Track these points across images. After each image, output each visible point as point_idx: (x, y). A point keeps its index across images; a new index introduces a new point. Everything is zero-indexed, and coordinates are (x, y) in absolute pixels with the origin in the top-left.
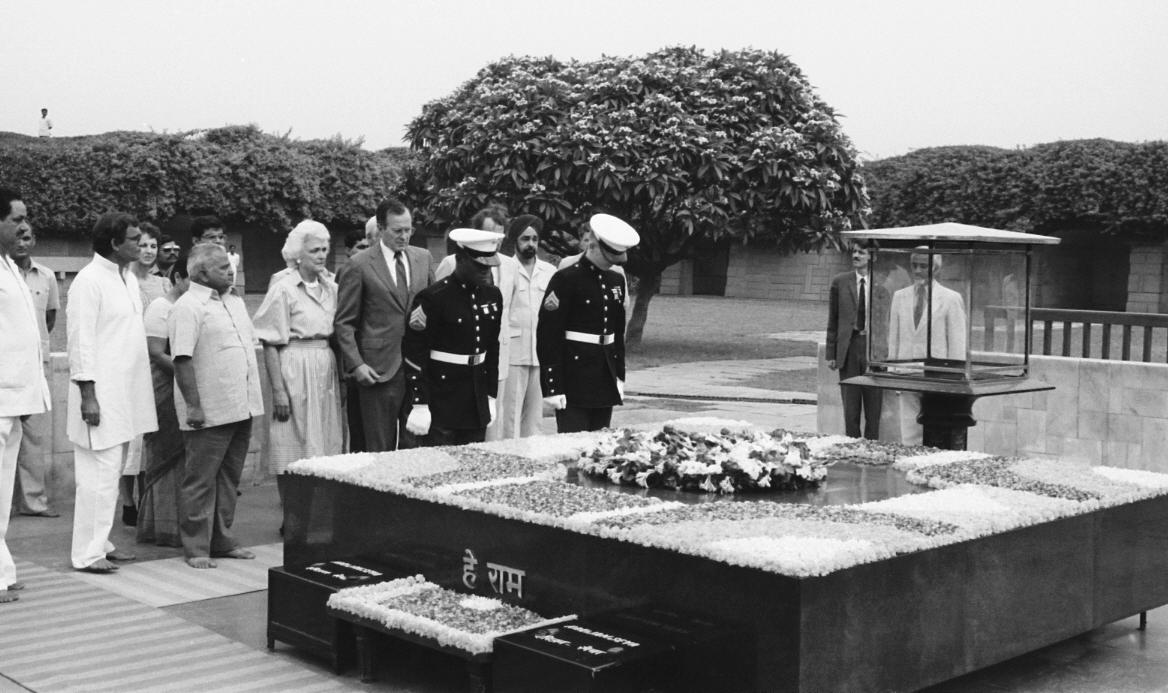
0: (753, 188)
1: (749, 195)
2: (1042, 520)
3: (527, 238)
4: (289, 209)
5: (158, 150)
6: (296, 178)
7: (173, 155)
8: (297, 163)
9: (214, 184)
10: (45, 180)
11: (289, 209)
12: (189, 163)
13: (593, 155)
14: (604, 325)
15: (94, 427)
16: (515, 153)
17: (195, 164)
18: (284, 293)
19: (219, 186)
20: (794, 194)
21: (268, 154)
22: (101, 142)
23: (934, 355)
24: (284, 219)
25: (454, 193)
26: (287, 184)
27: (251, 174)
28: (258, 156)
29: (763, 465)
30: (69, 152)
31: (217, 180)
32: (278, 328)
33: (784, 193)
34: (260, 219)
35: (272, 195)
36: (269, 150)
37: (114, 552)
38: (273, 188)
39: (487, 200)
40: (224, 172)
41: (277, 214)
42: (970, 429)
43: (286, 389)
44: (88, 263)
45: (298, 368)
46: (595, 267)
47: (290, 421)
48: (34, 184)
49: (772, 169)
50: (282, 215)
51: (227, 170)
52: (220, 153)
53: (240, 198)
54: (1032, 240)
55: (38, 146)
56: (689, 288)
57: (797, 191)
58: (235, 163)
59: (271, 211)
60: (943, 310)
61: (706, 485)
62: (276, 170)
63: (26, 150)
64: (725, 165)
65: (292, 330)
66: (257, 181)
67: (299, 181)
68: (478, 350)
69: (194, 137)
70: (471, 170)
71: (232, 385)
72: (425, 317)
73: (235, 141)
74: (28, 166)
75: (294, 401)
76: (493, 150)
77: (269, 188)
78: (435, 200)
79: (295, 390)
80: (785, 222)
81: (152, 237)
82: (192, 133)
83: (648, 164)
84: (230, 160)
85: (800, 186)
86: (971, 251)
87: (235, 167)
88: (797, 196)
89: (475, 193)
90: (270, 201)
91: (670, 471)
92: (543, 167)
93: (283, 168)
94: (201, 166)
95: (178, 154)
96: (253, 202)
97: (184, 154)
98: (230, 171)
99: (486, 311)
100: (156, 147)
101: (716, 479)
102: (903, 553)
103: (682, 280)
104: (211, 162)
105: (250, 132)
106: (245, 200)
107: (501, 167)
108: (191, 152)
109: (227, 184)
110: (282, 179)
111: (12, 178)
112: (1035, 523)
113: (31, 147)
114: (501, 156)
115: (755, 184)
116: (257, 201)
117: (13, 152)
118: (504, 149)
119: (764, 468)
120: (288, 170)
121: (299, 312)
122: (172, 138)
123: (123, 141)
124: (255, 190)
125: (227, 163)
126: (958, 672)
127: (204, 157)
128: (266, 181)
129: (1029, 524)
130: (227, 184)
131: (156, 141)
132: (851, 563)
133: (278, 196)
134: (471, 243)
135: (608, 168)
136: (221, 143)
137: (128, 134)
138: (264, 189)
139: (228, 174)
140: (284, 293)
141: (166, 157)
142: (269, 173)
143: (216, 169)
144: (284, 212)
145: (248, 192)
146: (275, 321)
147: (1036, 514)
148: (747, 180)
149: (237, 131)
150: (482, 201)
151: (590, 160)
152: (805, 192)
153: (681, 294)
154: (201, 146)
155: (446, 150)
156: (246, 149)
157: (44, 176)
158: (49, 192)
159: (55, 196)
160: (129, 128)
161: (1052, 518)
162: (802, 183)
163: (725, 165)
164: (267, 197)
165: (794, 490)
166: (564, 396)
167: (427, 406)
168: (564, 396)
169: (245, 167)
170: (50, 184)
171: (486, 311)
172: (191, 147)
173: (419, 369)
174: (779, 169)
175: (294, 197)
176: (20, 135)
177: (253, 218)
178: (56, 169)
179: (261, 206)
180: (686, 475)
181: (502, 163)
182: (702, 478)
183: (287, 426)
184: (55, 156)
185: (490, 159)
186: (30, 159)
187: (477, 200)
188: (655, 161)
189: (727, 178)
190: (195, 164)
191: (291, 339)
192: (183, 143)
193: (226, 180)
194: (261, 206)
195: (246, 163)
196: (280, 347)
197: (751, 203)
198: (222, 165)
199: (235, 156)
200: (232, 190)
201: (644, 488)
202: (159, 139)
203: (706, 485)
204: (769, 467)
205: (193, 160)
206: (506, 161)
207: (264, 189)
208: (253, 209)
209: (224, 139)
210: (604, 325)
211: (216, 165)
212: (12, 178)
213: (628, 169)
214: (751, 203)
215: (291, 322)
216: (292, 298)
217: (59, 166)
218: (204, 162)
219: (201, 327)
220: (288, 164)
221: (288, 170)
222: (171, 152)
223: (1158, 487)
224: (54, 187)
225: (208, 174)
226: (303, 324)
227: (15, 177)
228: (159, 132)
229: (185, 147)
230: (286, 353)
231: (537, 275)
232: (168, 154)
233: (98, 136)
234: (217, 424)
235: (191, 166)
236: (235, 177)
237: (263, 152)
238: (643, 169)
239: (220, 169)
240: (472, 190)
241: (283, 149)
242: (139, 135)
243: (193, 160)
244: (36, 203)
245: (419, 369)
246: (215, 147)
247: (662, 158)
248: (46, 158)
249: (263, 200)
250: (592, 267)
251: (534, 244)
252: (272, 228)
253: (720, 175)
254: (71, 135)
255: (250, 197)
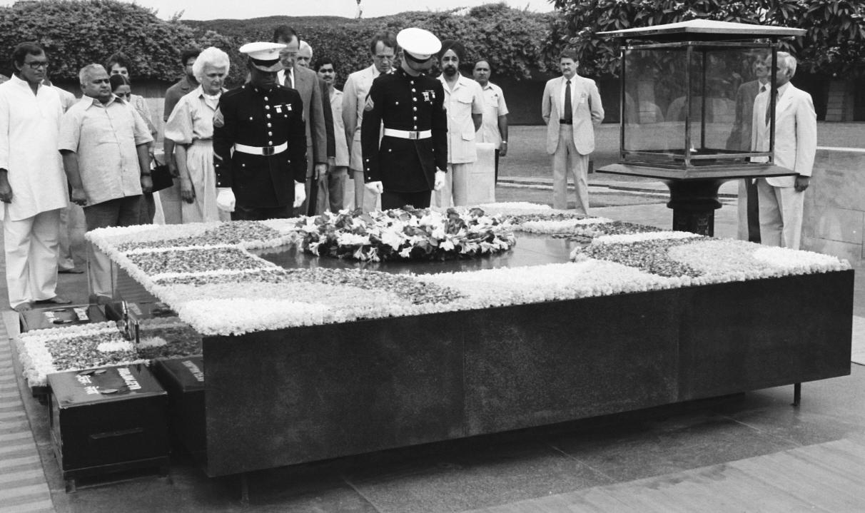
0: (818, 26)
1: (813, 31)
2: (590, 294)
3: (447, 59)
4: (528, 63)
5: (432, 24)
6: (532, 40)
7: (443, 27)
8: (533, 29)
9: (472, 46)
10: (355, 49)
11: (528, 63)
12: (454, 32)
13: (678, 4)
14: (414, 123)
15: (9, 204)
16: (618, 6)
17: (459, 32)
18: (187, 103)
19: (476, 48)
20: (853, 29)
21: (512, 23)
22: (393, 19)
23: (707, 146)
24: (524, 71)
25: (575, 40)
26: (525, 45)
27: (500, 38)
28: (505, 25)
29: (409, 238)
30: (371, 28)
31: (474, 43)
32: (182, 131)
33: (844, 28)
34: (508, 70)
35: (516, 54)
36: (514, 21)
37: (56, 297)
38: (516, 48)
39: (598, 44)
40: (480, 38)
41: (519, 68)
42: (716, 211)
43: (190, 178)
44: (6, 80)
45: (198, 160)
46: (407, 74)
47: (195, 203)
48: (349, 51)
49: (833, 8)
50: (523, 67)
51: (483, 36)
52: (479, 24)
53: (492, 56)
54: (772, 31)
55: (352, 24)
56: (851, 117)
57: (855, 26)
58: (488, 31)
59: (515, 65)
60: (793, 108)
61: (358, 254)
62: (518, 34)
63: (344, 28)
64: (791, 8)
65: (194, 132)
66: (504, 43)
67: (533, 41)
68: (271, 143)
69: (458, 14)
70: (588, 21)
71: (106, 172)
72: (222, 116)
73: (490, 15)
74: (343, 39)
75: (195, 187)
76: (601, 5)
77: (513, 48)
78: (567, 46)
79: (195, 180)
80: (849, 53)
81: (121, 66)
82: (456, 10)
83: (725, 10)
84: (485, 28)
85: (858, 22)
86: (690, 43)
87: (488, 34)
88: (855, 31)
89: (589, 39)
90: (514, 58)
91: (332, 242)
92: (640, 16)
93: (523, 33)
94: (463, 34)
95: (445, 26)
96: (501, 59)
97: (450, 26)
98: (485, 37)
99: (279, 111)
100: (431, 22)
101: (366, 249)
102: (367, 319)
103: (844, 110)
104: (471, 31)
105: (501, 7)
106: (496, 58)
107: (607, 18)
108: (455, 25)
109: (483, 46)
110: (522, 41)
111: (333, 48)
112: (582, 297)
113: (346, 25)
114: (607, 9)
115: (819, 22)
116: (504, 58)
117: (334, 30)
118: (609, 4)
119: (408, 241)
120: (526, 34)
121: (198, 119)
122: (442, 15)
123: (408, 18)
124: (502, 50)
125: (483, 31)
126: (456, 433)
127: (466, 27)
128: (510, 43)
129: (573, 297)
130: (483, 46)
131: (430, 17)
132: (282, 326)
133: (519, 53)
134: (253, 53)
135: (691, 14)
136: (480, 17)
137: (412, 13)
138: (509, 49)
139: (484, 39)
140: (187, 103)
141: (438, 28)
142: (513, 37)
143: (474, 36)
144: (524, 66)
145: (498, 52)
146: (180, 125)
147: (583, 289)
148: (812, 20)
149: (491, 8)
150: (595, 45)
151: (676, 8)
152: (861, 26)
153: (844, 120)
154: (464, 20)
155: (574, 7)
156: (497, 20)
157: (354, 45)
158: (357, 57)
159: (362, 59)
160: (415, 10)
161: (645, 289)
162: (859, 19)
163: (791, 8)
164: (511, 55)
165: (442, 261)
166: (380, 183)
167: (672, 210)
168: (380, 183)
169: (496, 34)
170: (358, 51)
171: (279, 111)
172: (456, 21)
173: (221, 158)
174: (839, 8)
175: (531, 54)
176: (341, 18)
177: (502, 70)
178: (362, 40)
179: (507, 61)
180: (343, 246)
181: (608, 15)
182: (355, 247)
183: (192, 206)
184: (361, 31)
185: (601, 11)
186: (345, 34)
187: (591, 44)
188: (731, 6)
189: (795, 18)
190: (459, 32)
191: (194, 140)
192: (451, 18)
193: (482, 43)
194: (507, 61)
195: (497, 30)
196: (187, 146)
197: (815, 38)
198: (479, 33)
199: (489, 25)
200: (486, 50)
201: (317, 256)
202: (433, 16)
203: (358, 254)
204: (413, 240)
205: (457, 29)
206: (610, 13)
207: (509, 49)
208: (502, 64)
209: (481, 14)
210: (414, 123)
211: (474, 33)
212: (333, 48)
213: (709, 14)
214: (815, 38)
215: (193, 127)
216: (191, 106)
217: (364, 38)
218: (465, 31)
219: (80, 130)
220: (526, 31)
221: (526, 34)
222: (441, 24)
223: (793, 267)
224: (361, 53)
225: (468, 40)
226: (201, 128)
227: (335, 47)
228: (434, 11)
229: (451, 21)
230: (191, 151)
231: (458, 89)
232: (439, 26)
233: (392, 16)
234: (98, 202)
235: (456, 35)
236: (488, 41)
237: (509, 22)
238: (721, 14)
239: (477, 37)
240: (588, 37)
241: (524, 19)
242: (418, 14)
243: (457, 29)
244: (349, 65)
245: (221, 158)
246: (474, 20)
247: (735, 4)
248: (356, 33)
249: (509, 57)
250: (404, 74)
251: (456, 64)
252: (516, 78)
253: (786, 16)
254: (377, 16)
255: (499, 55)
